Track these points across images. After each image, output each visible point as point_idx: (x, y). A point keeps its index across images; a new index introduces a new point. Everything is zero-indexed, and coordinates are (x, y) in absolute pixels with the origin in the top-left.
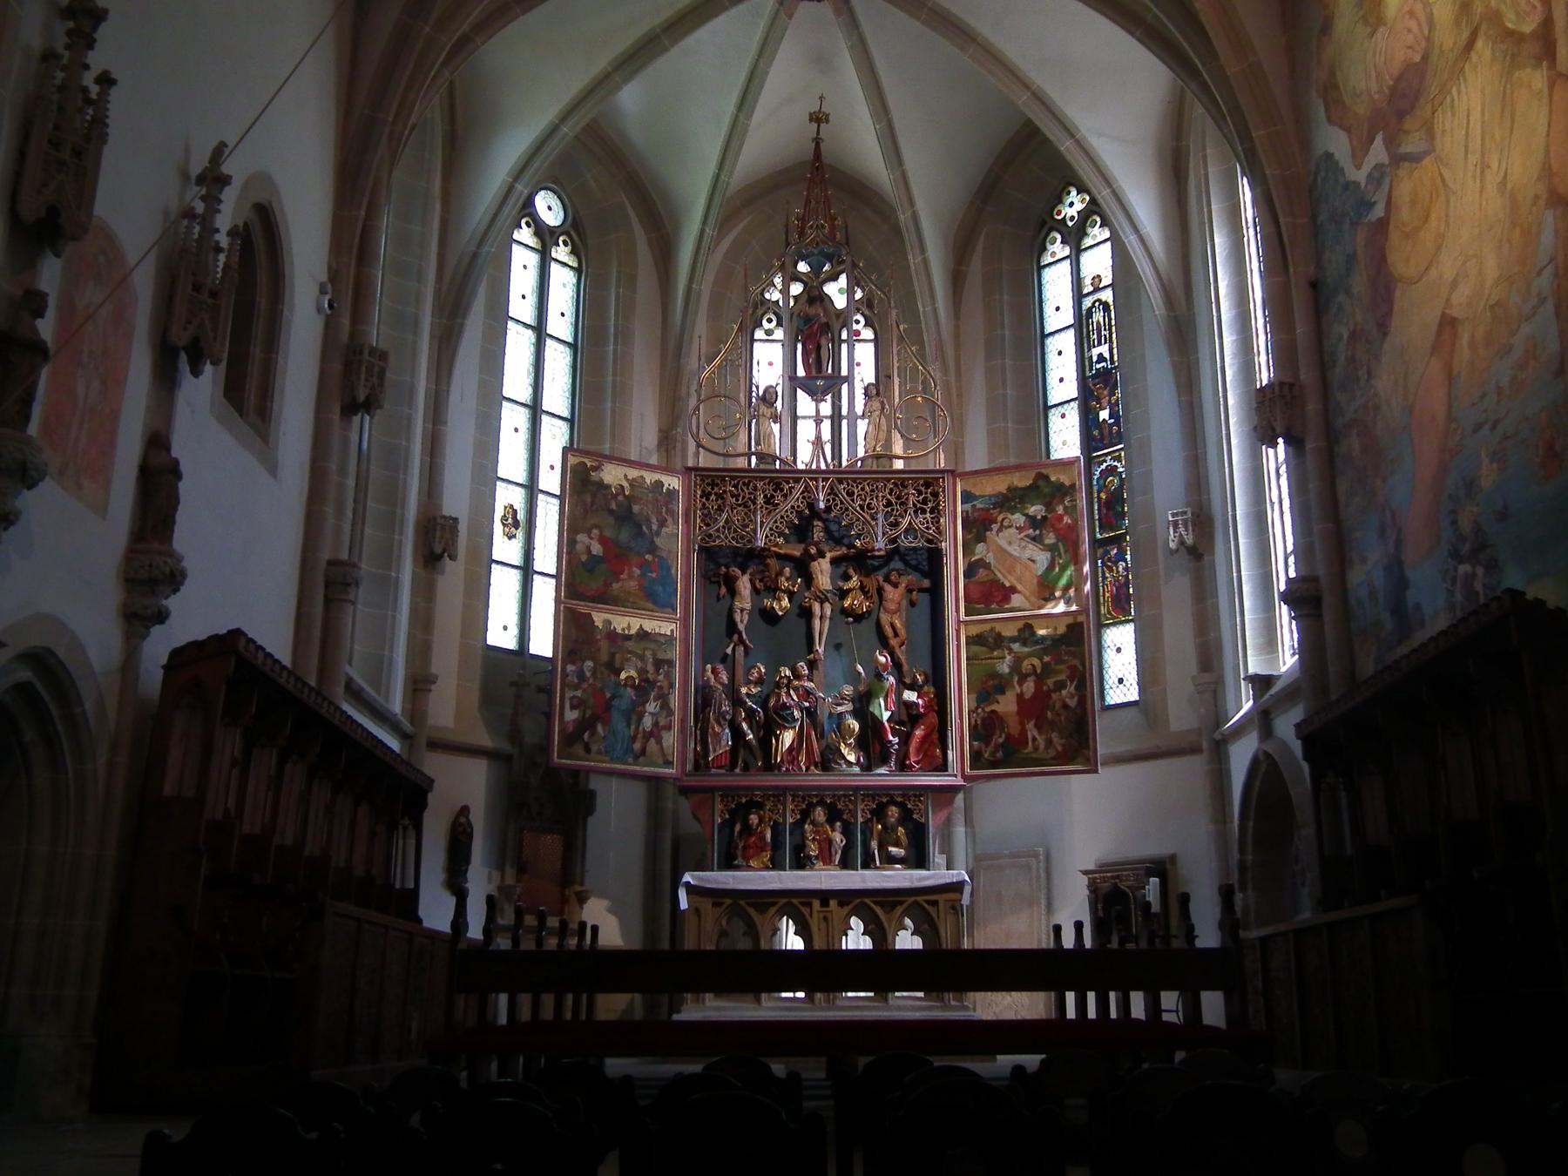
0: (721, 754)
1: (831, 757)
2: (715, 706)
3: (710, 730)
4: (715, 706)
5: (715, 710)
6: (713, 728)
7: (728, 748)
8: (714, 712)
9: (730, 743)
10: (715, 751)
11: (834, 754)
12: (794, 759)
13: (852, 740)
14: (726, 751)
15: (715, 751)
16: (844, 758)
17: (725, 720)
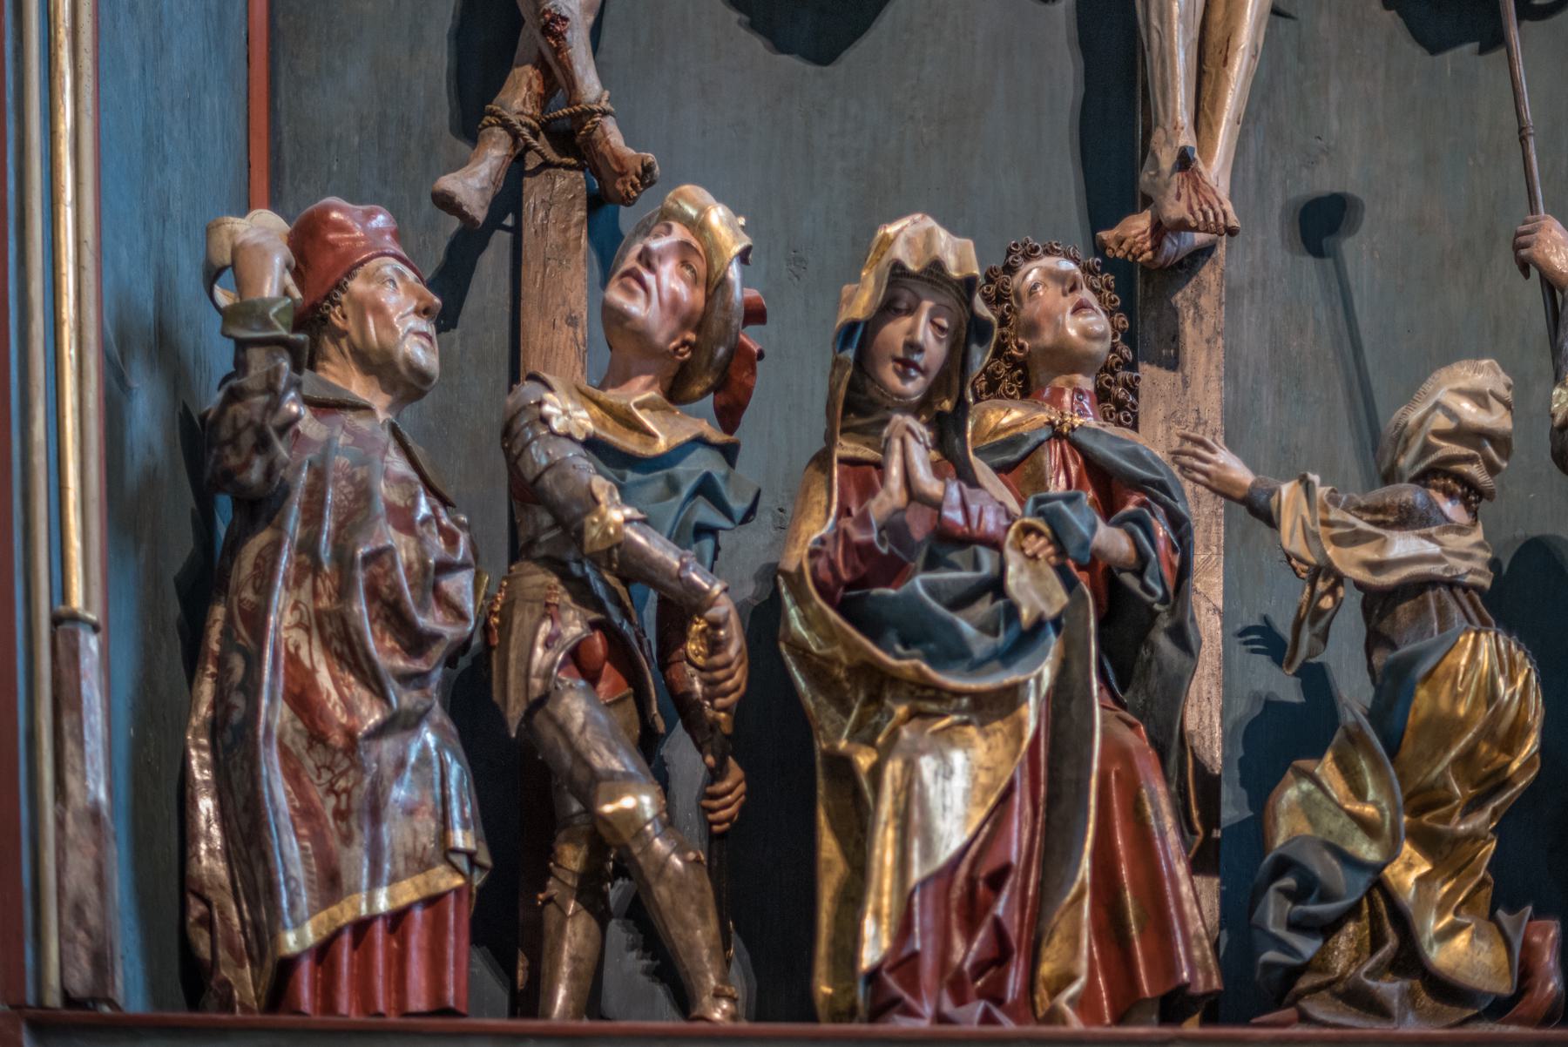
0: (398, 919)
1: (1308, 947)
2: (313, 515)
3: (275, 714)
4: (313, 515)
5: (308, 547)
6: (303, 700)
7: (445, 880)
8: (309, 564)
9: (460, 838)
10: (331, 884)
11: (1327, 929)
12: (999, 955)
13: (1481, 820)
14: (433, 901)
15: (331, 884)
16: (1410, 961)
17: (416, 642)
